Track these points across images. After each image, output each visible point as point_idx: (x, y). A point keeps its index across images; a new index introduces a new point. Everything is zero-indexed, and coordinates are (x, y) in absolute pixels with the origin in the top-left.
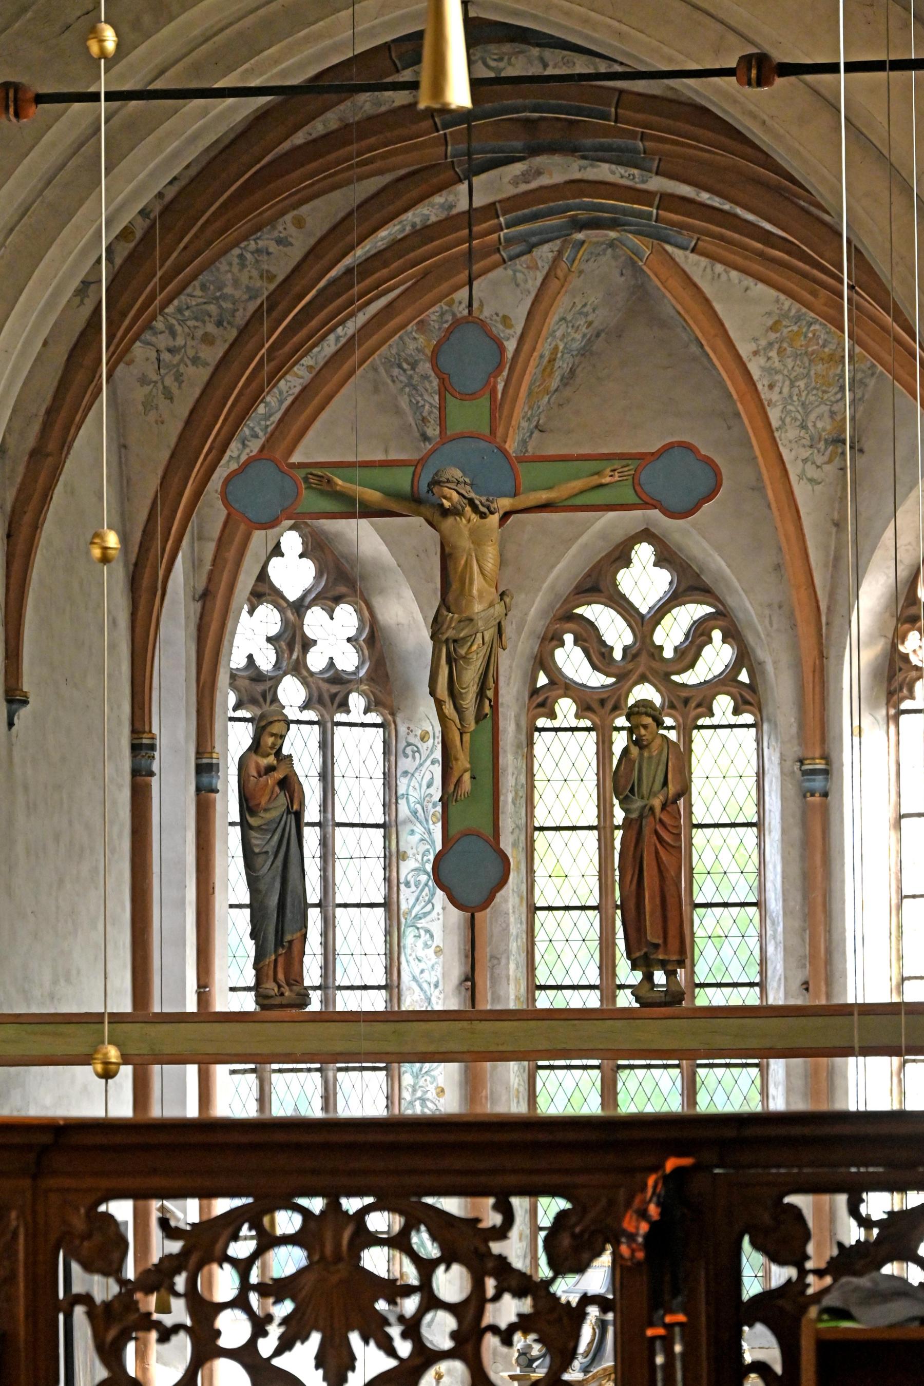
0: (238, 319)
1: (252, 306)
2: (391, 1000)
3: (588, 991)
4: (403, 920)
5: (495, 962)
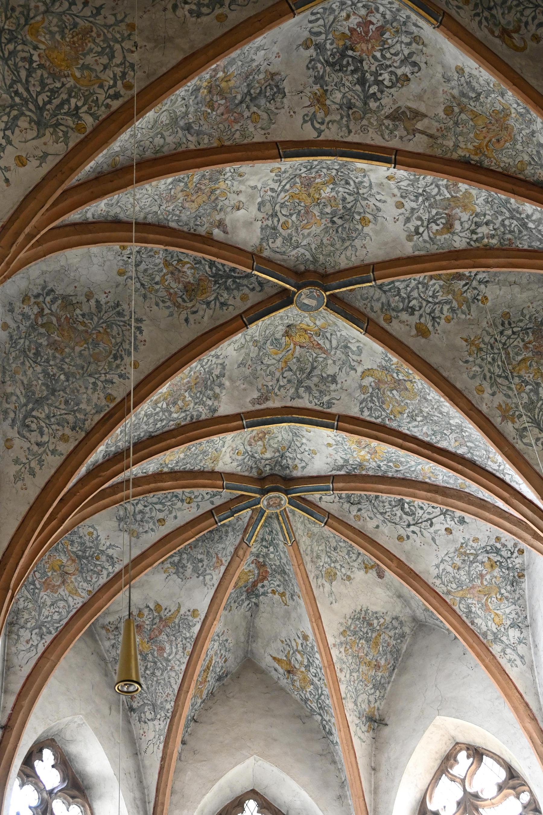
0: (86, 426)
1: (97, 418)
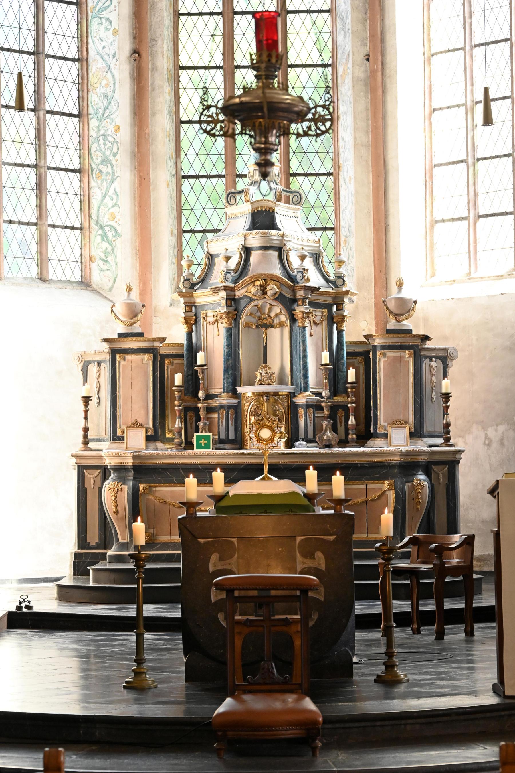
2: (82, 69)
3: (215, 70)
4: (90, 14)
5: (154, 43)
